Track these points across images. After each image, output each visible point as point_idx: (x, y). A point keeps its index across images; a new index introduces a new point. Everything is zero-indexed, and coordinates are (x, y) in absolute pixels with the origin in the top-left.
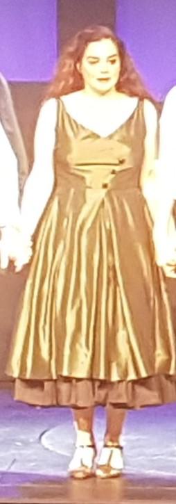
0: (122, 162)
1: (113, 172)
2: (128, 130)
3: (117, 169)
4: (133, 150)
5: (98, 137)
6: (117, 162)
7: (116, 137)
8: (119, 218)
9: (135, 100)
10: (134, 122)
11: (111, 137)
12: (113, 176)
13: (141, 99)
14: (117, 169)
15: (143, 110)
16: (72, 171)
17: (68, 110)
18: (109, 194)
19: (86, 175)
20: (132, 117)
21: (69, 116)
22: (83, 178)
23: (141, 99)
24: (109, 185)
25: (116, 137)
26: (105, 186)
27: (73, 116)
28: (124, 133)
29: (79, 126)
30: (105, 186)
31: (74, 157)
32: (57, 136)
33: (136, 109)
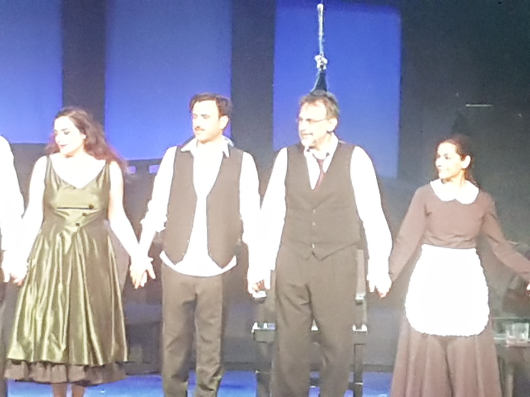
0: (91, 207)
1: (84, 215)
2: (98, 184)
3: (88, 212)
4: (101, 200)
5: (75, 188)
6: (87, 207)
7: (88, 189)
8: (88, 249)
9: (103, 162)
10: (103, 174)
11: (84, 189)
12: (84, 217)
13: (108, 163)
14: (88, 212)
15: (109, 170)
16: (55, 212)
17: (55, 166)
18: (81, 231)
19: (67, 217)
20: (100, 174)
21: (55, 173)
22: (64, 219)
23: (108, 163)
24: (81, 225)
25: (88, 189)
26: (78, 225)
27: (57, 172)
28: (95, 186)
29: (62, 181)
30: (78, 225)
31: (58, 201)
32: (46, 185)
33: (104, 167)
